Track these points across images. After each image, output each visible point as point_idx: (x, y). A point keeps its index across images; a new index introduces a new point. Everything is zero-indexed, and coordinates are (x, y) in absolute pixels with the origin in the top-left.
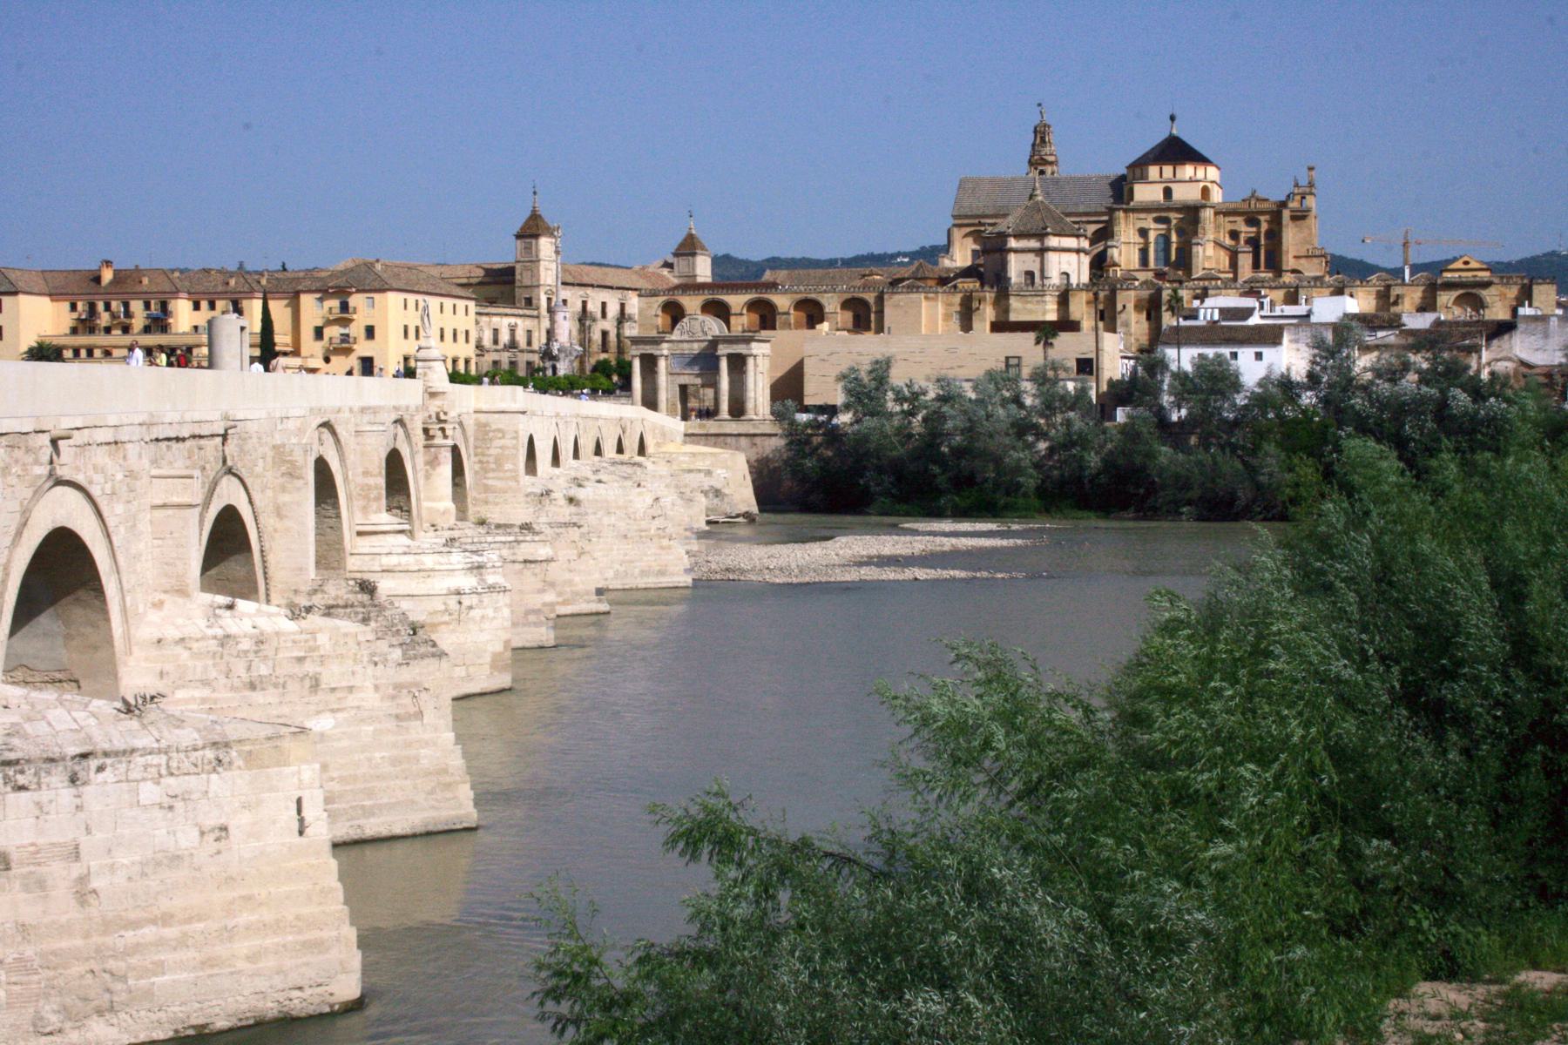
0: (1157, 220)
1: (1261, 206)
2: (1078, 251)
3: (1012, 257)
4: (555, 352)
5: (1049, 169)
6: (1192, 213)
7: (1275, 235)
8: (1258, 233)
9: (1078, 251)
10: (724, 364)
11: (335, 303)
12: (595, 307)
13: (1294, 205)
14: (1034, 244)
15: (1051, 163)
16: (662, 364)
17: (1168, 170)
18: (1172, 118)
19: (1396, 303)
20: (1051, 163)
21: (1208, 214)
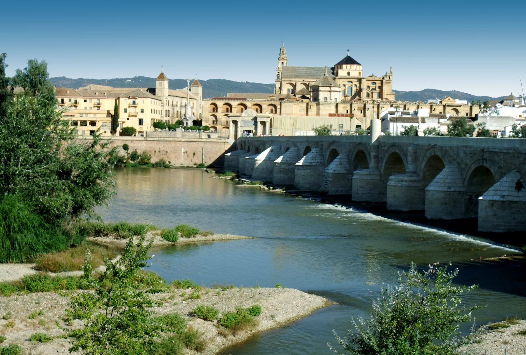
0: (348, 81)
1: (376, 79)
3: (321, 93)
4: (188, 118)
5: (285, 62)
6: (360, 80)
7: (381, 88)
8: (376, 87)
9: (340, 92)
10: (259, 125)
11: (131, 101)
12: (175, 103)
13: (386, 79)
14: (328, 89)
15: (286, 60)
16: (239, 124)
17: (349, 66)
18: (348, 51)
19: (434, 110)
20: (286, 60)
21: (363, 81)
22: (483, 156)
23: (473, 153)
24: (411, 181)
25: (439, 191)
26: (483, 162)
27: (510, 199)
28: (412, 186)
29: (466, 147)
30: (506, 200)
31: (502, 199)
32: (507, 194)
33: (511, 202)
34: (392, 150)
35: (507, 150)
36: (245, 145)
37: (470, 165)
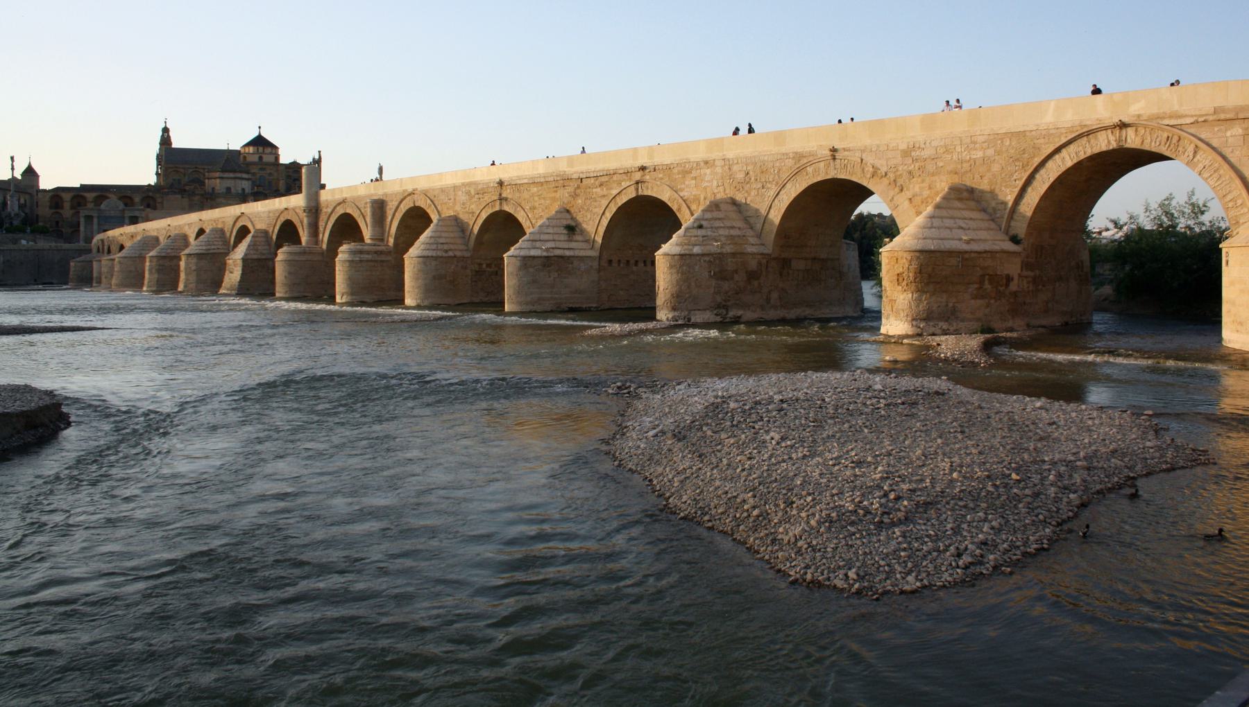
0: (261, 169)
2: (248, 179)
16: (95, 220)
17: (261, 149)
18: (260, 127)
22: (500, 195)
23: (482, 192)
24: (376, 252)
25: (428, 257)
26: (501, 204)
27: (558, 252)
28: (376, 261)
29: (470, 184)
30: (552, 255)
31: (545, 254)
32: (553, 246)
33: (562, 257)
34: (340, 211)
35: (544, 177)
36: (103, 245)
37: (478, 212)
